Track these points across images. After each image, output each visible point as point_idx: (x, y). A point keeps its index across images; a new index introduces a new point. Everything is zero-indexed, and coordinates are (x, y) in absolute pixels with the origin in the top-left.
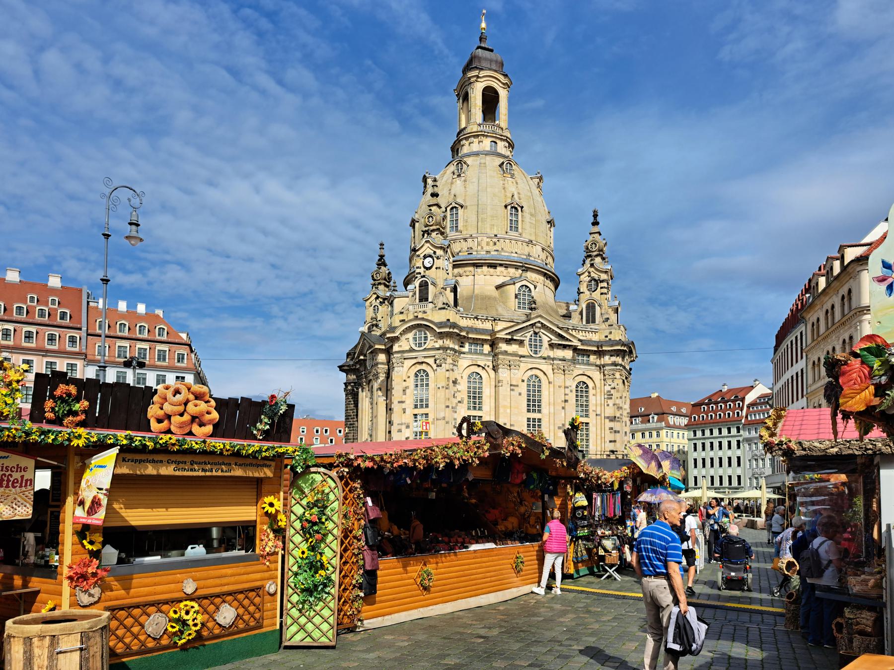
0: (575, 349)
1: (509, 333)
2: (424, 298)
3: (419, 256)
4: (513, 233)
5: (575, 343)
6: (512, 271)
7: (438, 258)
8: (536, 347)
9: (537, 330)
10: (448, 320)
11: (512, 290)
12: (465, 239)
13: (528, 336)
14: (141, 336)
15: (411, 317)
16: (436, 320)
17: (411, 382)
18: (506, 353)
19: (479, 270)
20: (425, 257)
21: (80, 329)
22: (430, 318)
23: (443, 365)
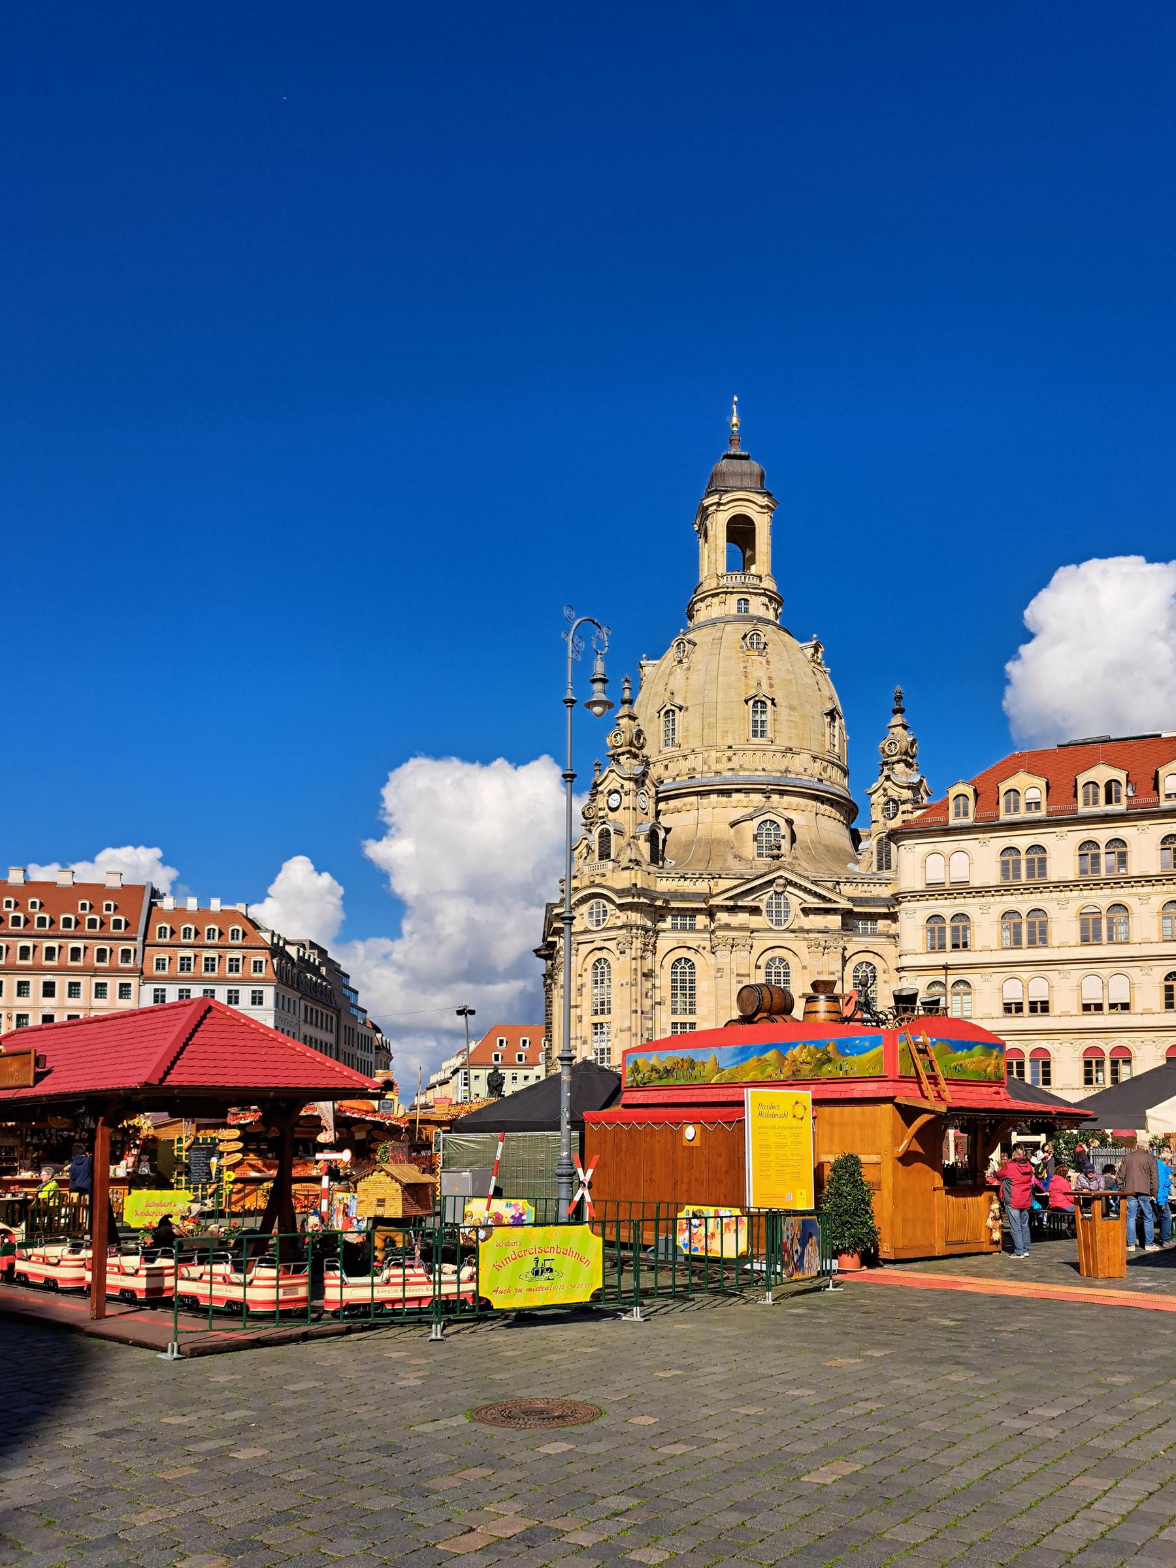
0: (847, 914)
1: (730, 898)
2: (605, 855)
3: (602, 792)
4: (756, 740)
5: (844, 904)
6: (757, 798)
7: (626, 794)
8: (778, 915)
9: (780, 890)
10: (635, 885)
11: (750, 828)
12: (685, 757)
13: (763, 900)
14: (210, 942)
15: (586, 882)
16: (618, 887)
17: (588, 978)
18: (727, 927)
19: (705, 801)
20: (610, 793)
21: (135, 939)
22: (609, 884)
23: (627, 951)
